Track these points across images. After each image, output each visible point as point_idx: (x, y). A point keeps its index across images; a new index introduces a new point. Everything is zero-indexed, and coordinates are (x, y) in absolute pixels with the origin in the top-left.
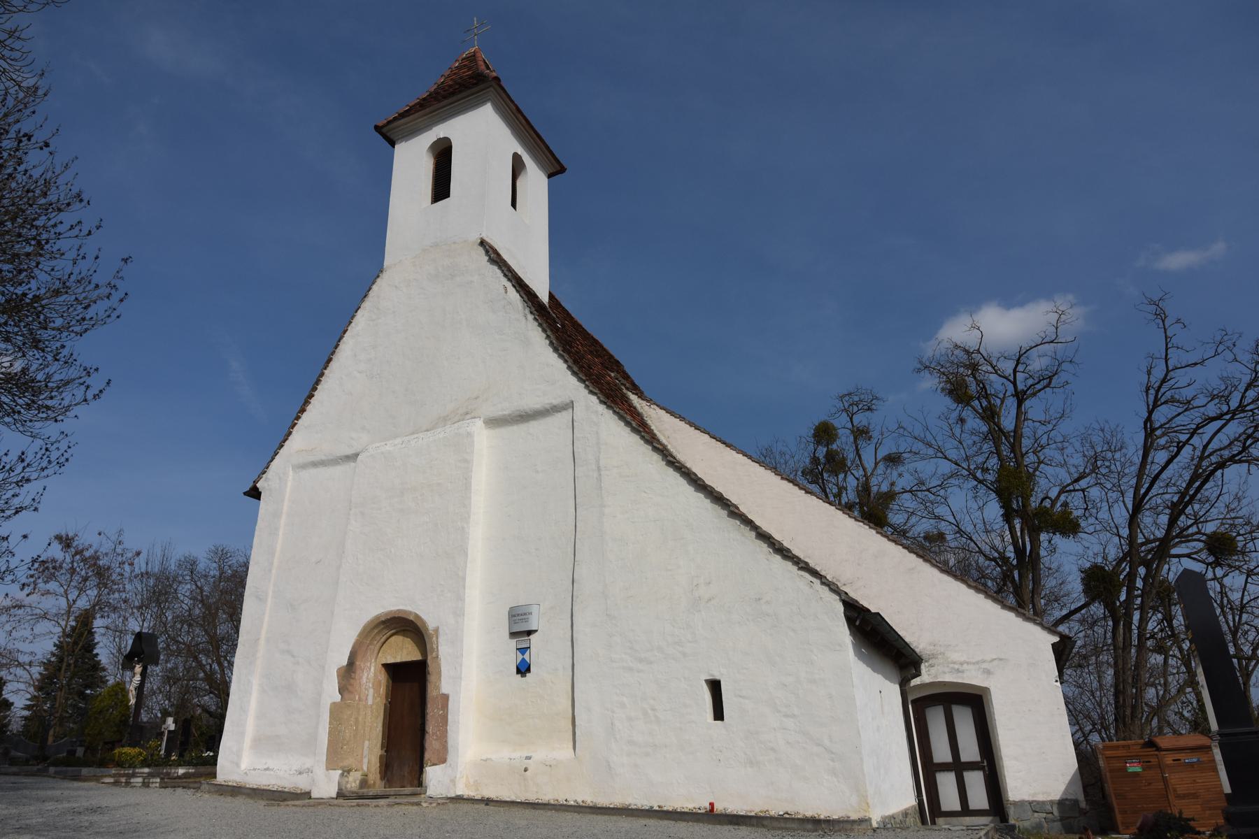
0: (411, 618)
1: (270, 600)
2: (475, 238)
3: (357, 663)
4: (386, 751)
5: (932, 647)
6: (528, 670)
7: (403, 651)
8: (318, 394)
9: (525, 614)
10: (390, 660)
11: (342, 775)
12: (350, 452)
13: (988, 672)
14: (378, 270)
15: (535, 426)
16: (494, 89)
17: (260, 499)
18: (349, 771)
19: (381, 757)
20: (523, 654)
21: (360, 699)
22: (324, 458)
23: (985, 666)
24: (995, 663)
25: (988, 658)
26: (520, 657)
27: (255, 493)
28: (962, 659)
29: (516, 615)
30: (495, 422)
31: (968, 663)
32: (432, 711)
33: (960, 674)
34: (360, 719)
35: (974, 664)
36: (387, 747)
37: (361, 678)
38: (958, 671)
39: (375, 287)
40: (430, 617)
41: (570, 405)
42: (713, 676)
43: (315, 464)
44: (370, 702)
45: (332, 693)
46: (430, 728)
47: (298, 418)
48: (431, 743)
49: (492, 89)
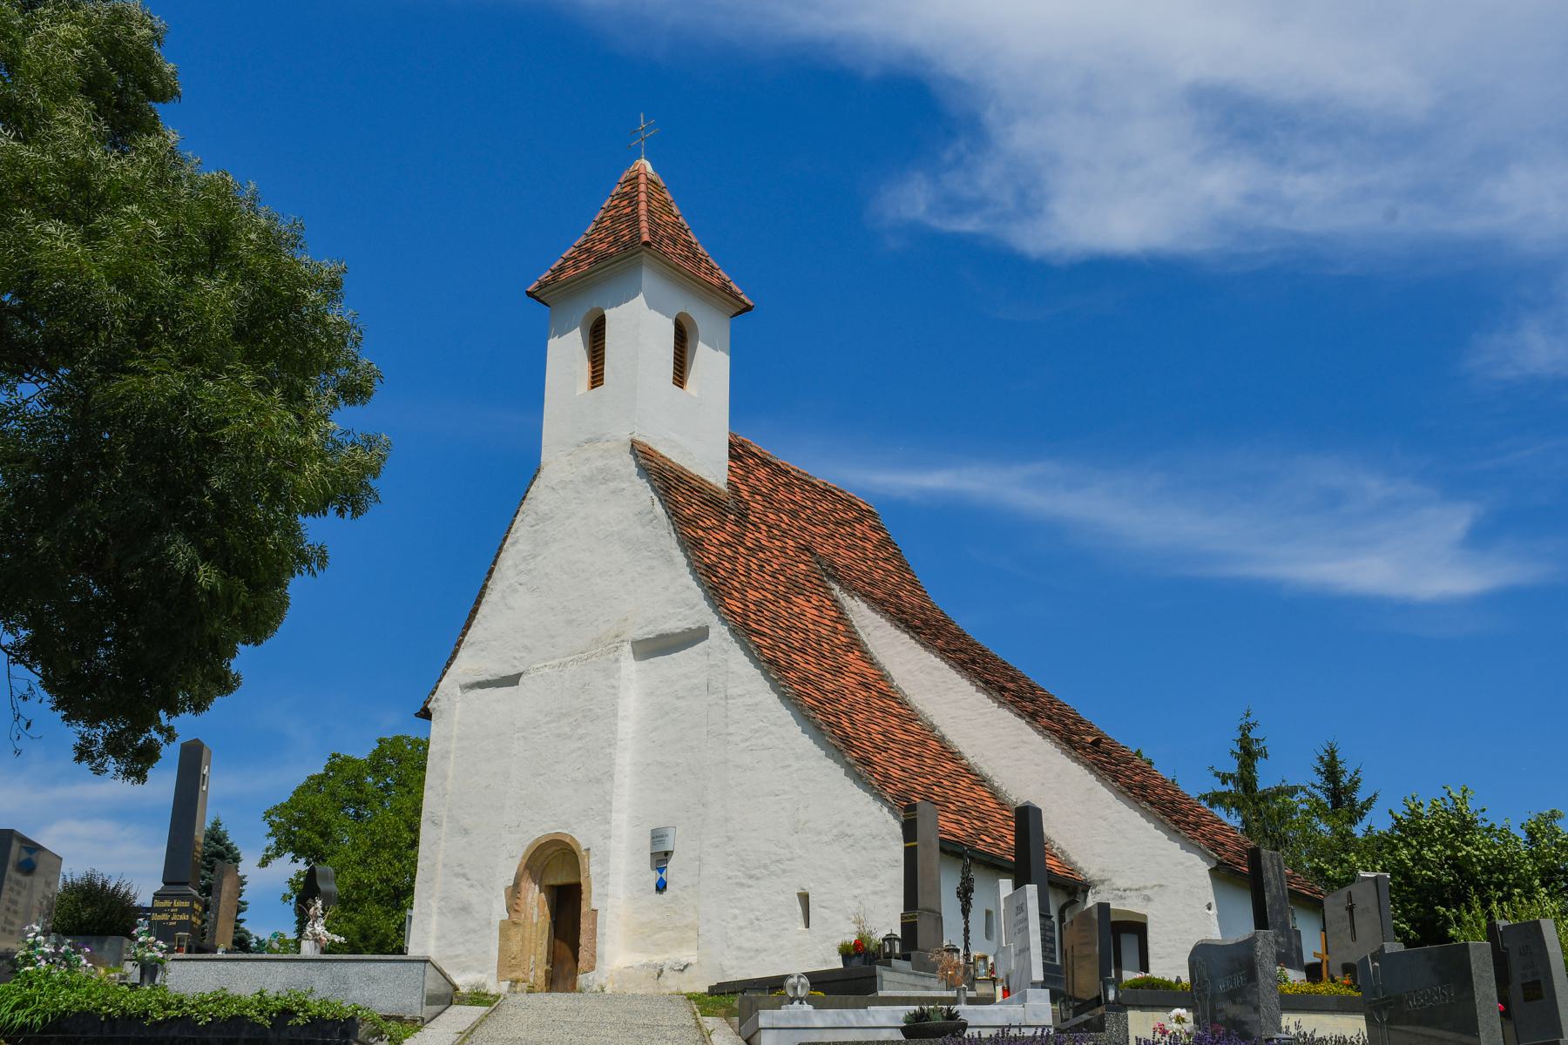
0: (567, 840)
1: (444, 824)
2: (625, 437)
3: (522, 884)
4: (551, 967)
5: (1101, 873)
6: (665, 887)
8: (483, 610)
9: (662, 836)
10: (553, 882)
11: (511, 985)
12: (512, 672)
14: (533, 470)
16: (646, 251)
17: (430, 719)
18: (517, 981)
19: (547, 971)
20: (661, 873)
21: (526, 917)
22: (490, 678)
24: (1156, 889)
25: (1148, 884)
26: (659, 875)
27: (426, 714)
28: (1126, 886)
29: (657, 836)
31: (1130, 890)
33: (1122, 901)
34: (526, 935)
35: (1136, 890)
36: (553, 963)
37: (526, 898)
38: (1121, 898)
39: (532, 488)
42: (803, 889)
44: (535, 920)
45: (500, 911)
46: (583, 940)
47: (464, 634)
49: (643, 253)
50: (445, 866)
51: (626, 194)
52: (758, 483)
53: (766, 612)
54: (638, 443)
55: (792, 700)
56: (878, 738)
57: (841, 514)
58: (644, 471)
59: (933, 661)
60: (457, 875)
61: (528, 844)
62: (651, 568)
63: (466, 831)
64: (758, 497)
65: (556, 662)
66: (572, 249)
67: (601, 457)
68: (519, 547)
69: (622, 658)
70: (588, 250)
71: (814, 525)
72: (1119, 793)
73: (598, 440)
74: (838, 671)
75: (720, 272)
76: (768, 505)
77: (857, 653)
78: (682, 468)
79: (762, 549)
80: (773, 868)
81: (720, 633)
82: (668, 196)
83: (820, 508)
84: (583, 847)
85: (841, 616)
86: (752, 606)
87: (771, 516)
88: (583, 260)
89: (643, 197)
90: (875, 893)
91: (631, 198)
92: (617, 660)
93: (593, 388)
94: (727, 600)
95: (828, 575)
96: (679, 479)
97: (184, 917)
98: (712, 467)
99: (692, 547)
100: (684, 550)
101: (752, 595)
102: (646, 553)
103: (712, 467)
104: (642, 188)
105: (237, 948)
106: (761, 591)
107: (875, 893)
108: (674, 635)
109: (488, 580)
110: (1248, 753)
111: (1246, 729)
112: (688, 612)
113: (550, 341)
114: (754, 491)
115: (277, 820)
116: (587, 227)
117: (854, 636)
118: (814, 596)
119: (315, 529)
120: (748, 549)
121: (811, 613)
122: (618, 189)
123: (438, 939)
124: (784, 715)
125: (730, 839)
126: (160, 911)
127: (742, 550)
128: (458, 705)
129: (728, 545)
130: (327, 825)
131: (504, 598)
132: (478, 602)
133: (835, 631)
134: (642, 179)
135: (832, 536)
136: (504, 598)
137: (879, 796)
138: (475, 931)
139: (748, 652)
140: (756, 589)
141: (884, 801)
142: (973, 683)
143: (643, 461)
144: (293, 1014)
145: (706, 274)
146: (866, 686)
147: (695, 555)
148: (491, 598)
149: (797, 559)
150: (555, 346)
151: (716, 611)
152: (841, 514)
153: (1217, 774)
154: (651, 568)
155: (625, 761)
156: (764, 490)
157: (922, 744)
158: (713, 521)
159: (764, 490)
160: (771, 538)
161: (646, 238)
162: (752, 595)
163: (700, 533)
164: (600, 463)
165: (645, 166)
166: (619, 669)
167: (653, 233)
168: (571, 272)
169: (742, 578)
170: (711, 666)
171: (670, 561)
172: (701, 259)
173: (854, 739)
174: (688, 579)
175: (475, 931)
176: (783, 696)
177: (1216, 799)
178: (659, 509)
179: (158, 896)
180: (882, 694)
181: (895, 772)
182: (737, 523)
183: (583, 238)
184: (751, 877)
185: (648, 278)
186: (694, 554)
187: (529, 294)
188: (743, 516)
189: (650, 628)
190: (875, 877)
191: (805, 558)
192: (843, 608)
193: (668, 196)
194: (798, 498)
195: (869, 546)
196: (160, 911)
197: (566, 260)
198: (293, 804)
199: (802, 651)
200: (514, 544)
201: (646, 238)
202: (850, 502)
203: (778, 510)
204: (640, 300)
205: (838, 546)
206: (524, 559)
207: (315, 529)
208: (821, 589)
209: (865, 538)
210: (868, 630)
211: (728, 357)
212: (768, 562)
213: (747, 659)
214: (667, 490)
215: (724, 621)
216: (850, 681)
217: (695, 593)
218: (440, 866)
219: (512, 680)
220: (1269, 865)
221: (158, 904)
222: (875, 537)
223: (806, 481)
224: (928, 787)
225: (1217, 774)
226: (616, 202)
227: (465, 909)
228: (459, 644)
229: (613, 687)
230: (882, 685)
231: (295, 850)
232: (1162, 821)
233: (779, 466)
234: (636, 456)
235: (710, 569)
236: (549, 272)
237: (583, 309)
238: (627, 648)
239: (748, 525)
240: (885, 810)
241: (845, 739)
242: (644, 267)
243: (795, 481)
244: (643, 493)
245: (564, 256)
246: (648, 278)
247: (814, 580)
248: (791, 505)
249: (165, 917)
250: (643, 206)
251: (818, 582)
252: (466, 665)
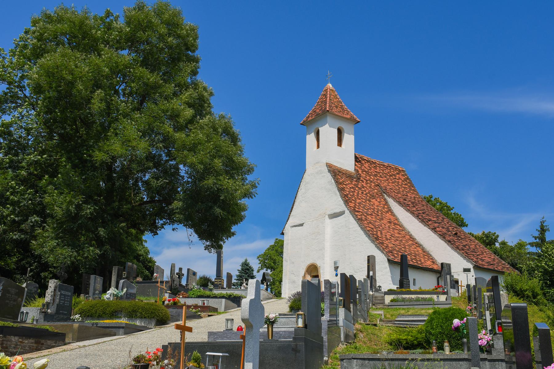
1: (288, 261)
2: (325, 162)
8: (294, 207)
10: (313, 275)
13: (459, 275)
14: (304, 171)
23: (458, 273)
27: (283, 234)
29: (335, 263)
43: (295, 226)
47: (290, 213)
50: (289, 272)
51: (325, 94)
52: (365, 168)
53: (361, 205)
54: (328, 163)
55: (363, 229)
56: (388, 237)
57: (392, 173)
58: (329, 171)
59: (408, 214)
60: (292, 274)
61: (307, 265)
62: (332, 196)
63: (293, 263)
64: (364, 172)
65: (311, 220)
66: (311, 111)
67: (320, 167)
68: (302, 191)
69: (326, 219)
70: (315, 111)
71: (382, 178)
72: (452, 248)
73: (319, 163)
75: (351, 113)
76: (367, 174)
77: (390, 213)
78: (341, 168)
79: (363, 187)
80: (360, 270)
81: (347, 212)
82: (336, 93)
83: (385, 172)
84: (319, 266)
85: (386, 203)
86: (357, 204)
87: (368, 177)
88: (313, 115)
89: (328, 95)
90: (382, 275)
91: (325, 95)
92: (324, 220)
93: (318, 148)
94: (350, 204)
95: (384, 192)
96: (339, 172)
97: (220, 283)
99: (341, 190)
100: (339, 191)
101: (358, 201)
102: (330, 192)
104: (328, 93)
105: (215, 283)
106: (361, 200)
107: (382, 275)
108: (337, 213)
109: (295, 199)
110: (543, 230)
111: (542, 223)
112: (340, 207)
113: (307, 136)
114: (363, 171)
115: (261, 259)
116: (315, 104)
117: (389, 208)
118: (378, 199)
119: (244, 201)
120: (359, 188)
121: (376, 203)
122: (323, 93)
123: (289, 289)
124: (362, 232)
125: (351, 263)
126: (216, 282)
127: (357, 189)
128: (290, 231)
129: (353, 188)
130: (275, 260)
131: (299, 204)
132: (293, 205)
133: (384, 208)
134: (329, 90)
135: (388, 180)
136: (299, 204)
137: (382, 252)
138: (296, 287)
139: (354, 217)
140: (360, 199)
141: (384, 253)
142: (418, 220)
143: (329, 168)
144: (231, 296)
145: (346, 115)
146: (390, 222)
147: (341, 192)
148: (296, 204)
149: (374, 189)
150: (308, 137)
151: (346, 206)
152: (392, 173)
153: (533, 237)
154: (332, 196)
155: (328, 245)
156: (366, 170)
158: (349, 182)
159: (366, 170)
160: (366, 184)
161: (328, 109)
162: (358, 201)
163: (344, 186)
164: (319, 169)
165: (330, 85)
166: (325, 222)
167: (330, 106)
168: (310, 118)
169: (356, 197)
170: (346, 221)
171: (336, 194)
172: (345, 110)
173: (380, 238)
174: (340, 199)
175: (296, 287)
176: (361, 228)
177: (532, 244)
178: (333, 181)
179: (215, 279)
180: (395, 224)
181: (390, 245)
182: (356, 181)
183: (314, 107)
184: (355, 272)
185: (329, 119)
186: (341, 192)
187: (301, 124)
188: (358, 179)
189: (332, 211)
190: (382, 271)
191: (377, 188)
192: (387, 201)
193: (336, 93)
194: (378, 170)
195: (400, 181)
196: (216, 282)
197: (310, 114)
198: (265, 254)
199: (371, 215)
200: (301, 190)
201: (328, 109)
202: (396, 168)
203: (370, 175)
204: (327, 125)
205: (389, 182)
206: (303, 194)
207: (244, 201)
208: (381, 196)
209: (399, 179)
210: (393, 207)
211: (354, 136)
212: (365, 191)
213: (353, 219)
214: (335, 176)
215: (348, 209)
216: (385, 221)
217: (342, 202)
218: (288, 271)
219: (302, 225)
220: (446, 266)
221: (216, 280)
222: (403, 178)
223: (382, 165)
225: (533, 237)
226: (322, 97)
227: (294, 282)
228: (289, 216)
229: (324, 226)
230: (396, 222)
231: (266, 267)
232: (462, 255)
233: (373, 162)
234: (327, 167)
235: (346, 196)
236: (306, 118)
237: (314, 127)
238: (327, 216)
239: (360, 181)
240: (384, 255)
241: (377, 239)
242: (328, 117)
243: (378, 165)
244: (329, 177)
245: (319, 98)
246: (329, 119)
247: (379, 194)
248: (375, 173)
249: (217, 283)
250: (328, 98)
251: (380, 194)
252: (291, 222)
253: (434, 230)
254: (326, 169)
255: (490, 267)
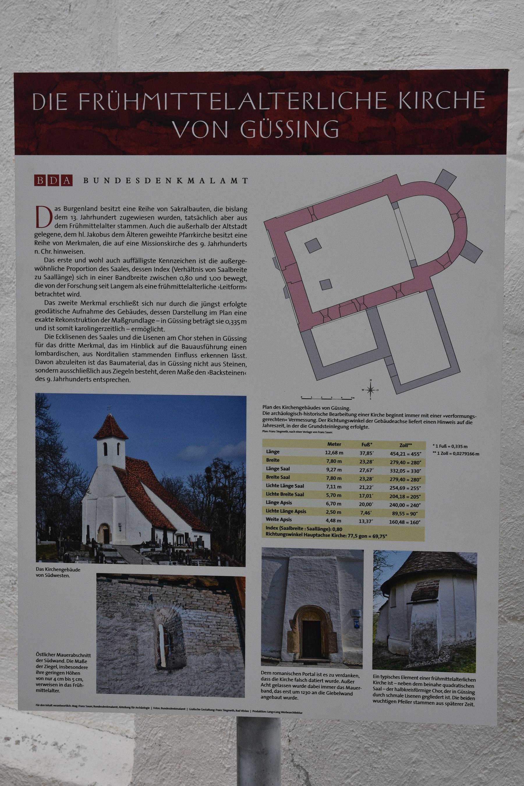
7: (105, 528)
15: (121, 498)
29: (119, 524)
30: (116, 497)
32: (110, 535)
40: (109, 524)
41: (125, 496)
45: (97, 533)
48: (110, 539)
74: (143, 500)
81: (127, 496)
85: (143, 489)
98: (122, 466)
103: (122, 466)
133: (142, 492)
157: (155, 510)
224: (155, 518)
244: (114, 474)
253: (170, 506)
254: (112, 470)
255: (199, 528)
